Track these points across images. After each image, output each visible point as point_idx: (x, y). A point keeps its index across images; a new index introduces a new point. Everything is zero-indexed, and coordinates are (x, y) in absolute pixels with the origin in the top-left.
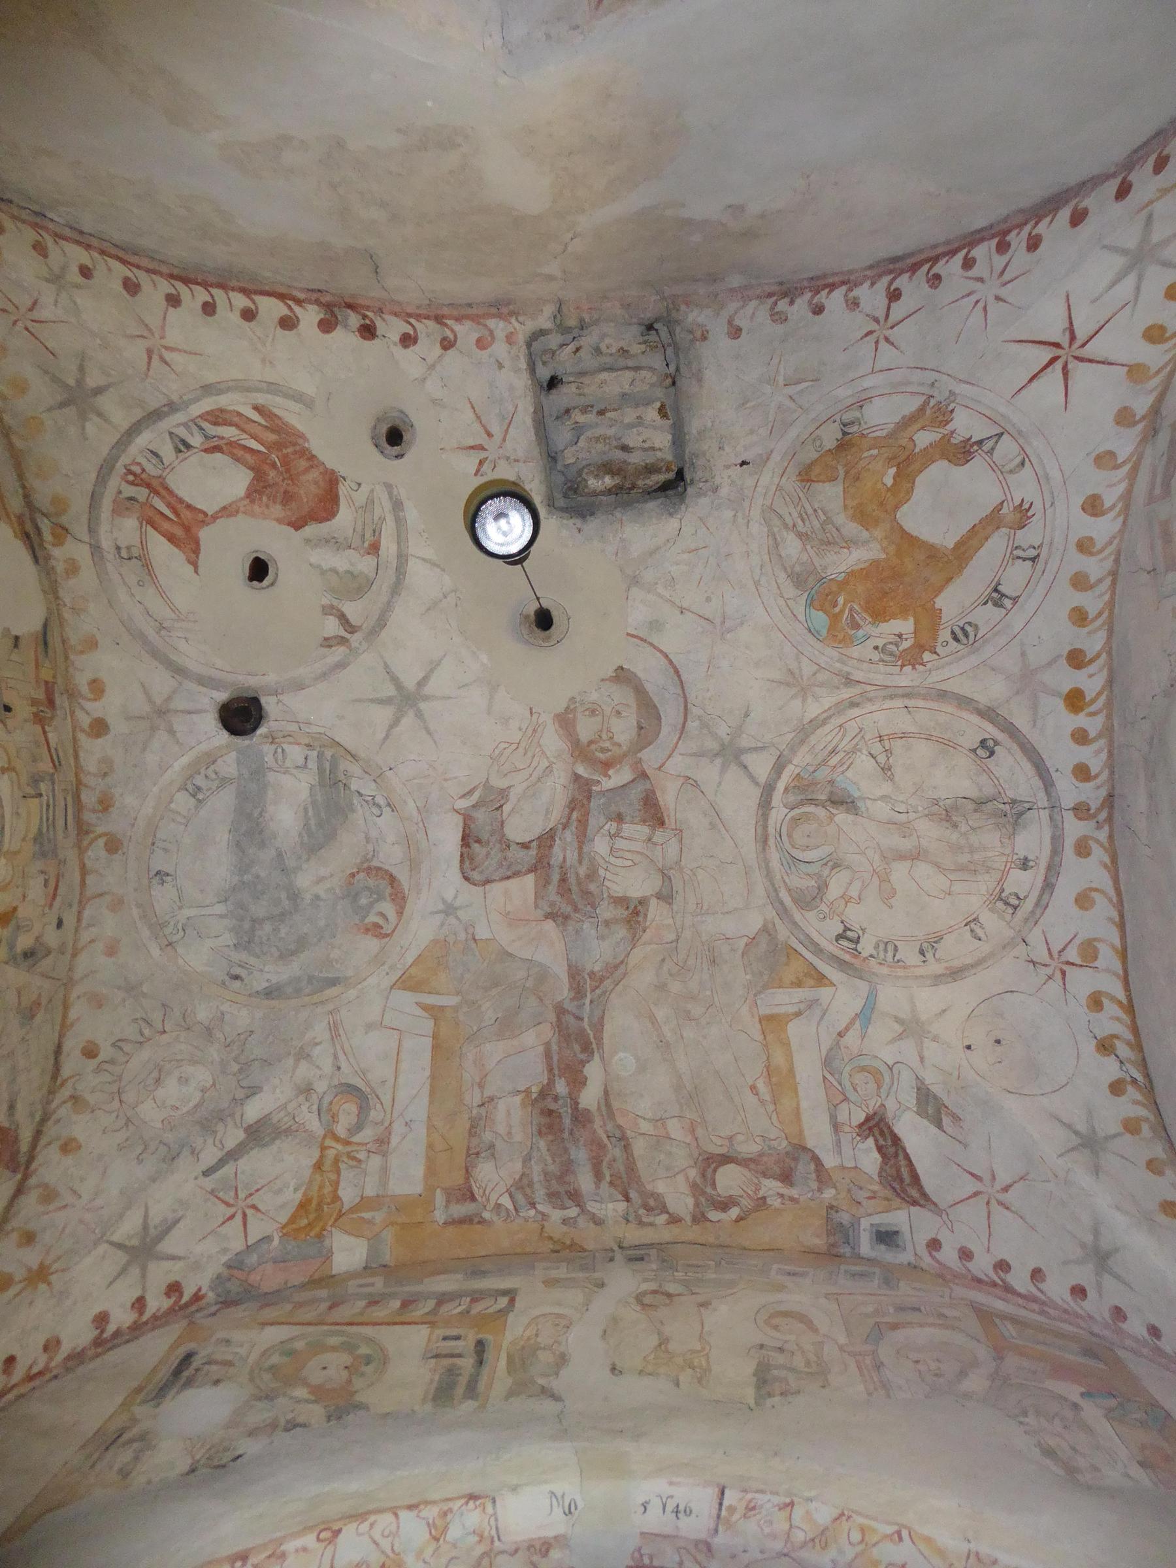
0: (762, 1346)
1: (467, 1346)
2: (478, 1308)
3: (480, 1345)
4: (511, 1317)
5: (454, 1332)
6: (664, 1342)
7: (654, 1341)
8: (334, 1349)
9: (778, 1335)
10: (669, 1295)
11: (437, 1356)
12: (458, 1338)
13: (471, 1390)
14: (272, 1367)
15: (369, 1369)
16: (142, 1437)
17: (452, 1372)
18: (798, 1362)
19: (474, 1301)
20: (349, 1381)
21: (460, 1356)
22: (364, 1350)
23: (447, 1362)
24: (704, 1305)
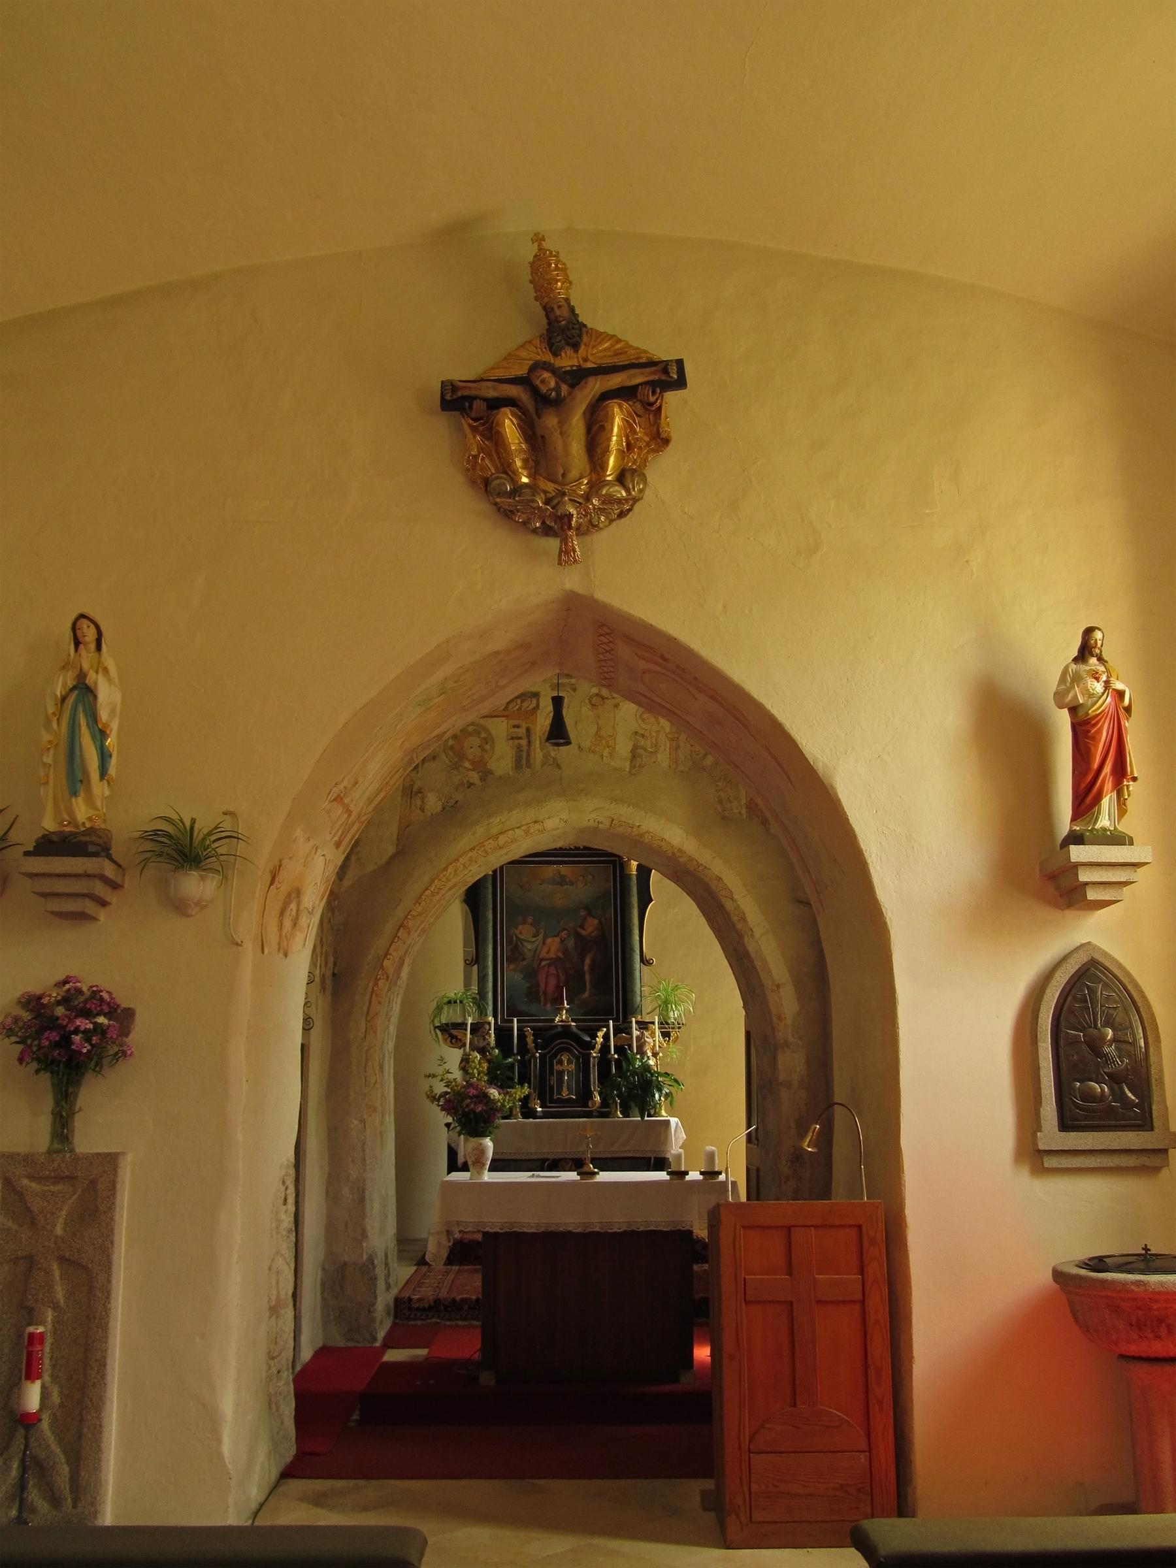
0: (636, 733)
1: (522, 731)
2: (525, 704)
3: (528, 730)
4: (539, 712)
5: (517, 722)
6: (599, 729)
7: (594, 729)
8: (470, 734)
9: (643, 726)
10: (603, 698)
11: (512, 738)
12: (518, 727)
13: (529, 765)
14: (452, 747)
15: (487, 747)
16: (420, 791)
17: (519, 747)
18: (648, 745)
19: (523, 701)
20: (482, 757)
21: (520, 738)
22: (483, 735)
23: (517, 742)
24: (616, 706)
